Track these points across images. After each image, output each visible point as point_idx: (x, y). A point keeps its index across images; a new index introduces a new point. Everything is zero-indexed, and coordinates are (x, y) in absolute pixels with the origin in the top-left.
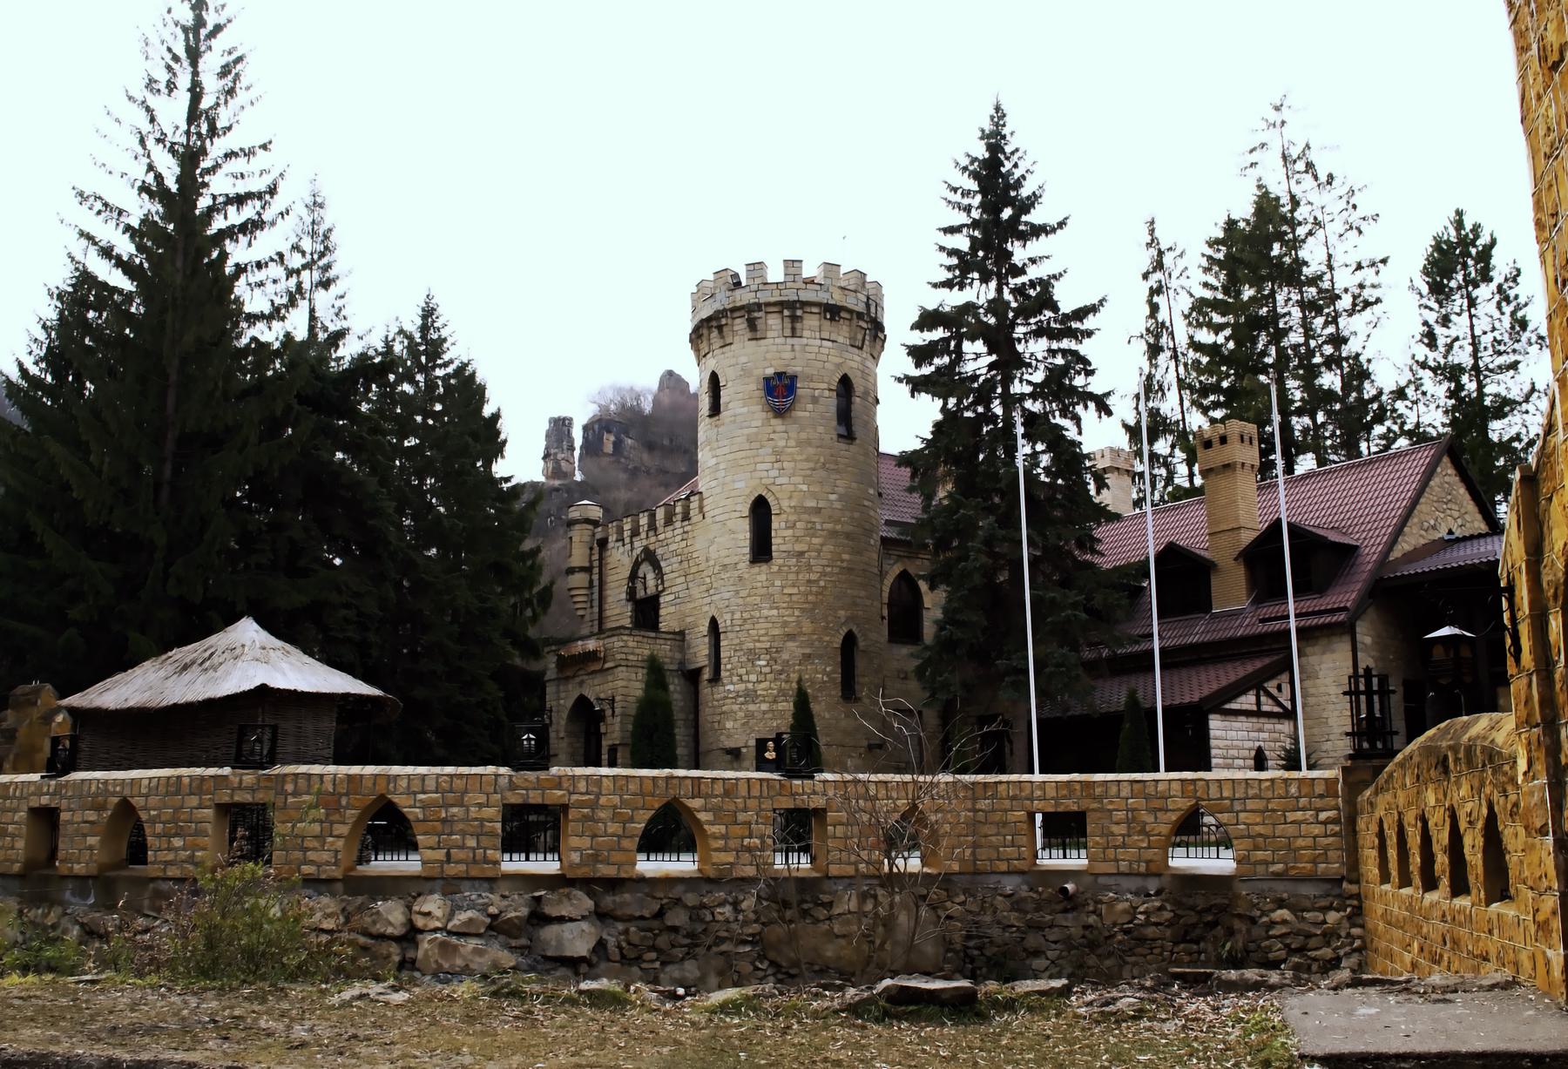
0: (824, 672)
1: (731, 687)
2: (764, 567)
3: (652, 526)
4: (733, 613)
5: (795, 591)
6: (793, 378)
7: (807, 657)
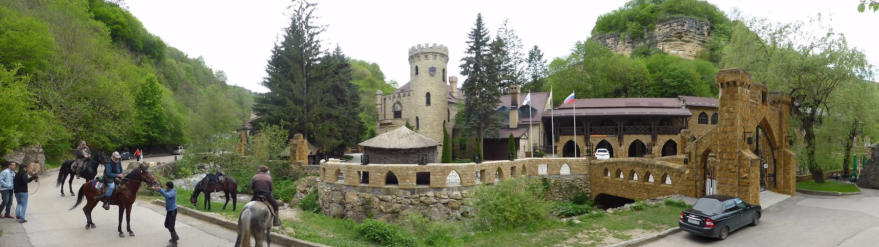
3: (399, 96)
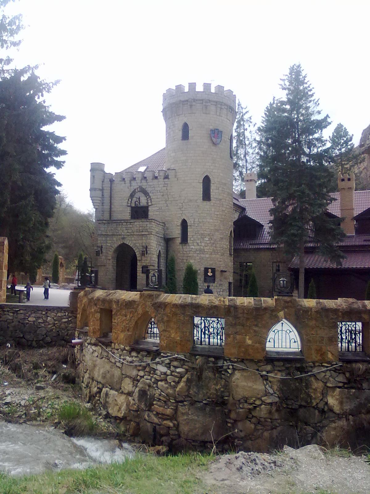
2: (208, 203)
4: (194, 219)
5: (218, 213)
7: (222, 238)
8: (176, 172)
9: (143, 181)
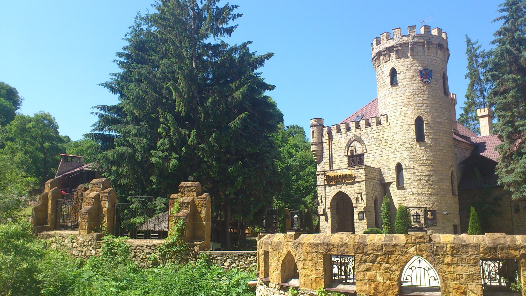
0: (447, 186)
1: (410, 190)
3: (358, 126)
6: (431, 71)
7: (442, 179)
8: (387, 117)
9: (357, 130)
